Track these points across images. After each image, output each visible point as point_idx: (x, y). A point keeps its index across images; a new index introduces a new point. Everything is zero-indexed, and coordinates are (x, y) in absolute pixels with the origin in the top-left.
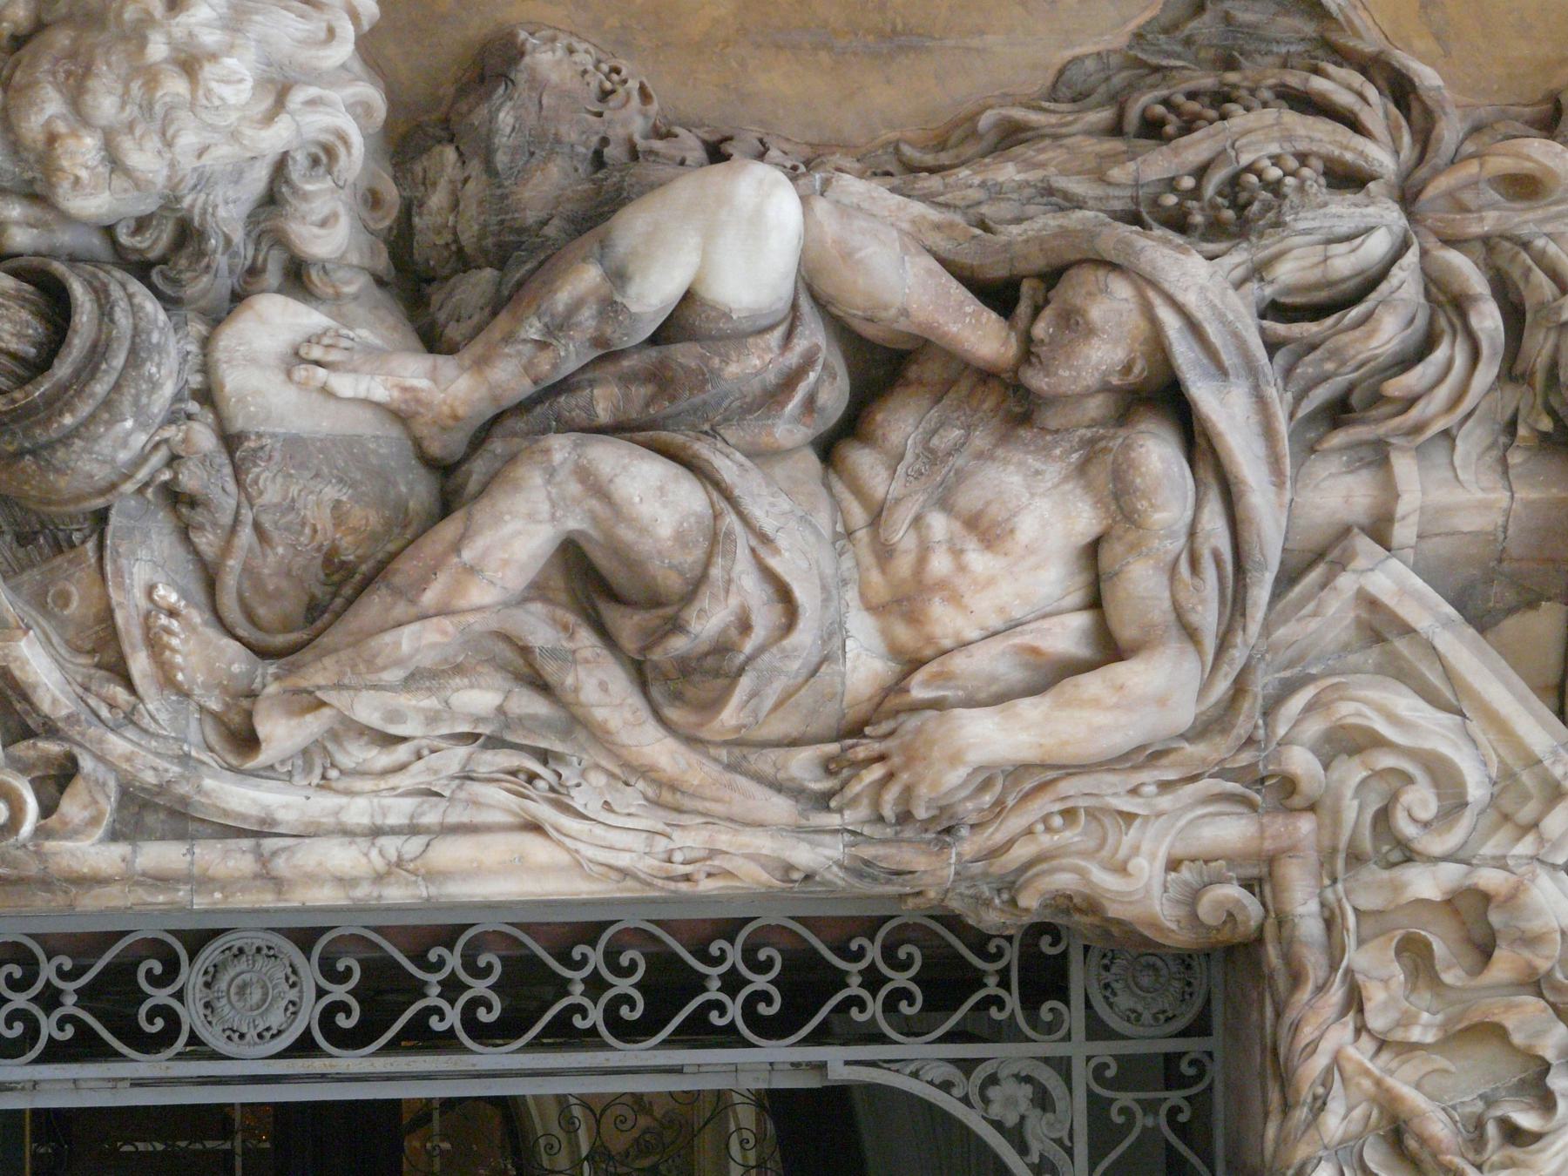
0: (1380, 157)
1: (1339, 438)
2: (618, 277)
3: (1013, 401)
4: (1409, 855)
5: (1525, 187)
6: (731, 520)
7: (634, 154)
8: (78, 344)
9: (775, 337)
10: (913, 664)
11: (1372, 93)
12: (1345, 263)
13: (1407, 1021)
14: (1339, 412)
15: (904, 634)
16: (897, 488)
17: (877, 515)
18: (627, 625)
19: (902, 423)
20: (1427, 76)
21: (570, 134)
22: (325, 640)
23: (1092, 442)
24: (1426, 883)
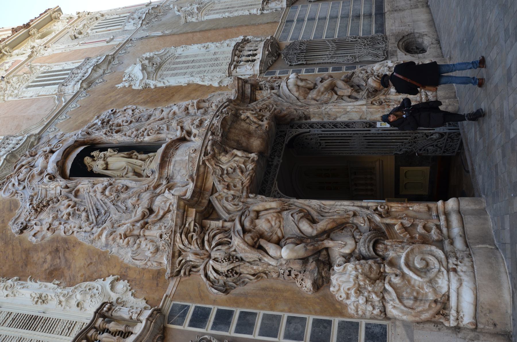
0: (211, 262)
1: (227, 229)
2: (305, 247)
3: (261, 235)
4: (233, 195)
5: (196, 254)
6: (296, 223)
7: (300, 272)
8: (372, 242)
9: (288, 242)
10: (279, 212)
11: (209, 273)
12: (219, 247)
13: (238, 181)
14: (226, 231)
15: (280, 215)
16: (277, 229)
17: (280, 227)
18: (310, 217)
19: (275, 237)
20: (203, 276)
21: (308, 273)
22: (344, 221)
23: (254, 229)
24: (232, 192)
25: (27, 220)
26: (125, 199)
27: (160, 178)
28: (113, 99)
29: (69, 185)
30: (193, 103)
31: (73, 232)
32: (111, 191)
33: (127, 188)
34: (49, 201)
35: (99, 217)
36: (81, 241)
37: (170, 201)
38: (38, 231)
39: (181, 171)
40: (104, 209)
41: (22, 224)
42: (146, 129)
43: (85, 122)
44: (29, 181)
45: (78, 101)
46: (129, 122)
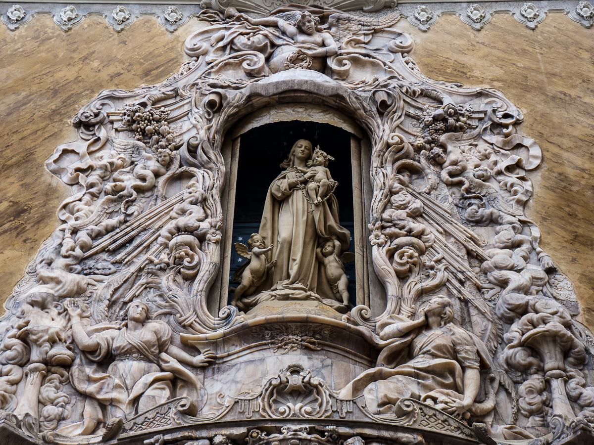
25: (111, 118)
26: (158, 288)
27: (214, 343)
28: (573, 93)
29: (200, 151)
30: (544, 321)
31: (64, 222)
32: (178, 246)
33: (191, 279)
34: (159, 134)
35: (104, 256)
36: (42, 247)
37: (123, 396)
38: (78, 154)
39: (233, 387)
40: (129, 254)
41: (96, 115)
42: (420, 235)
43: (460, 74)
44: (226, 64)
45: (561, 11)
46: (456, 179)
